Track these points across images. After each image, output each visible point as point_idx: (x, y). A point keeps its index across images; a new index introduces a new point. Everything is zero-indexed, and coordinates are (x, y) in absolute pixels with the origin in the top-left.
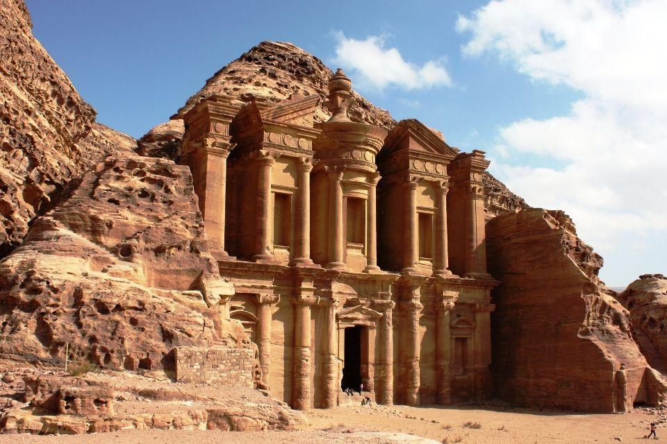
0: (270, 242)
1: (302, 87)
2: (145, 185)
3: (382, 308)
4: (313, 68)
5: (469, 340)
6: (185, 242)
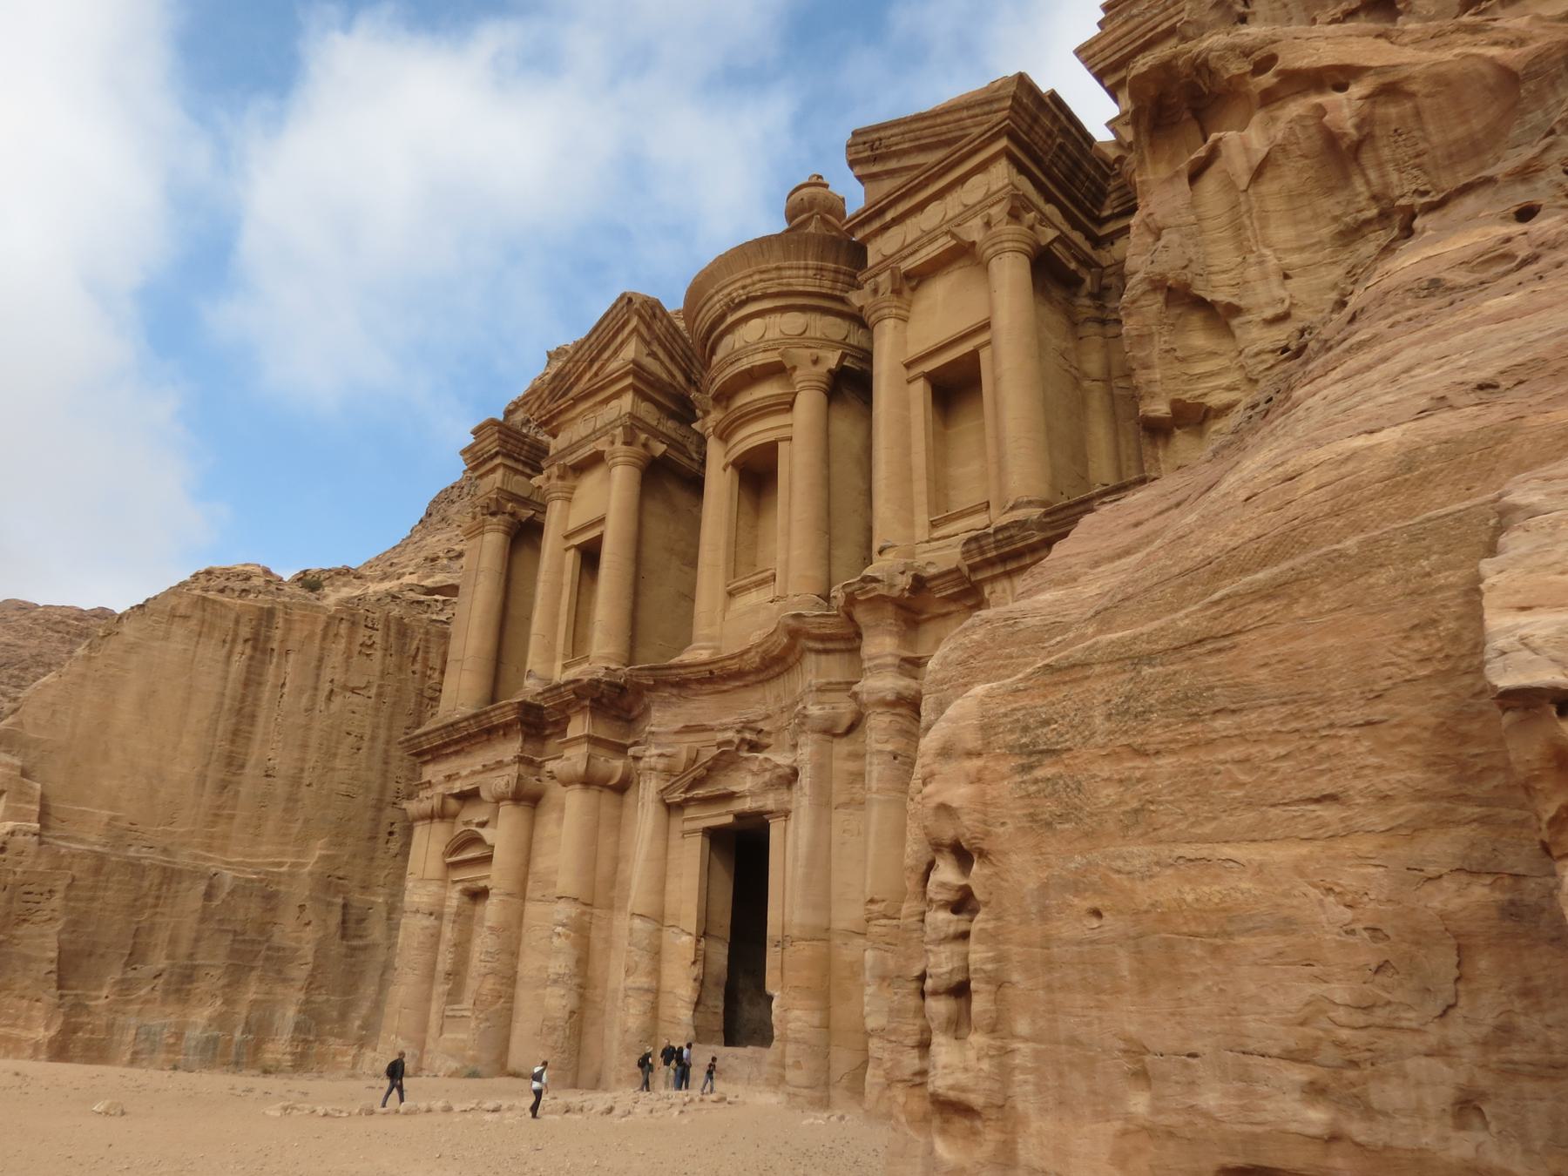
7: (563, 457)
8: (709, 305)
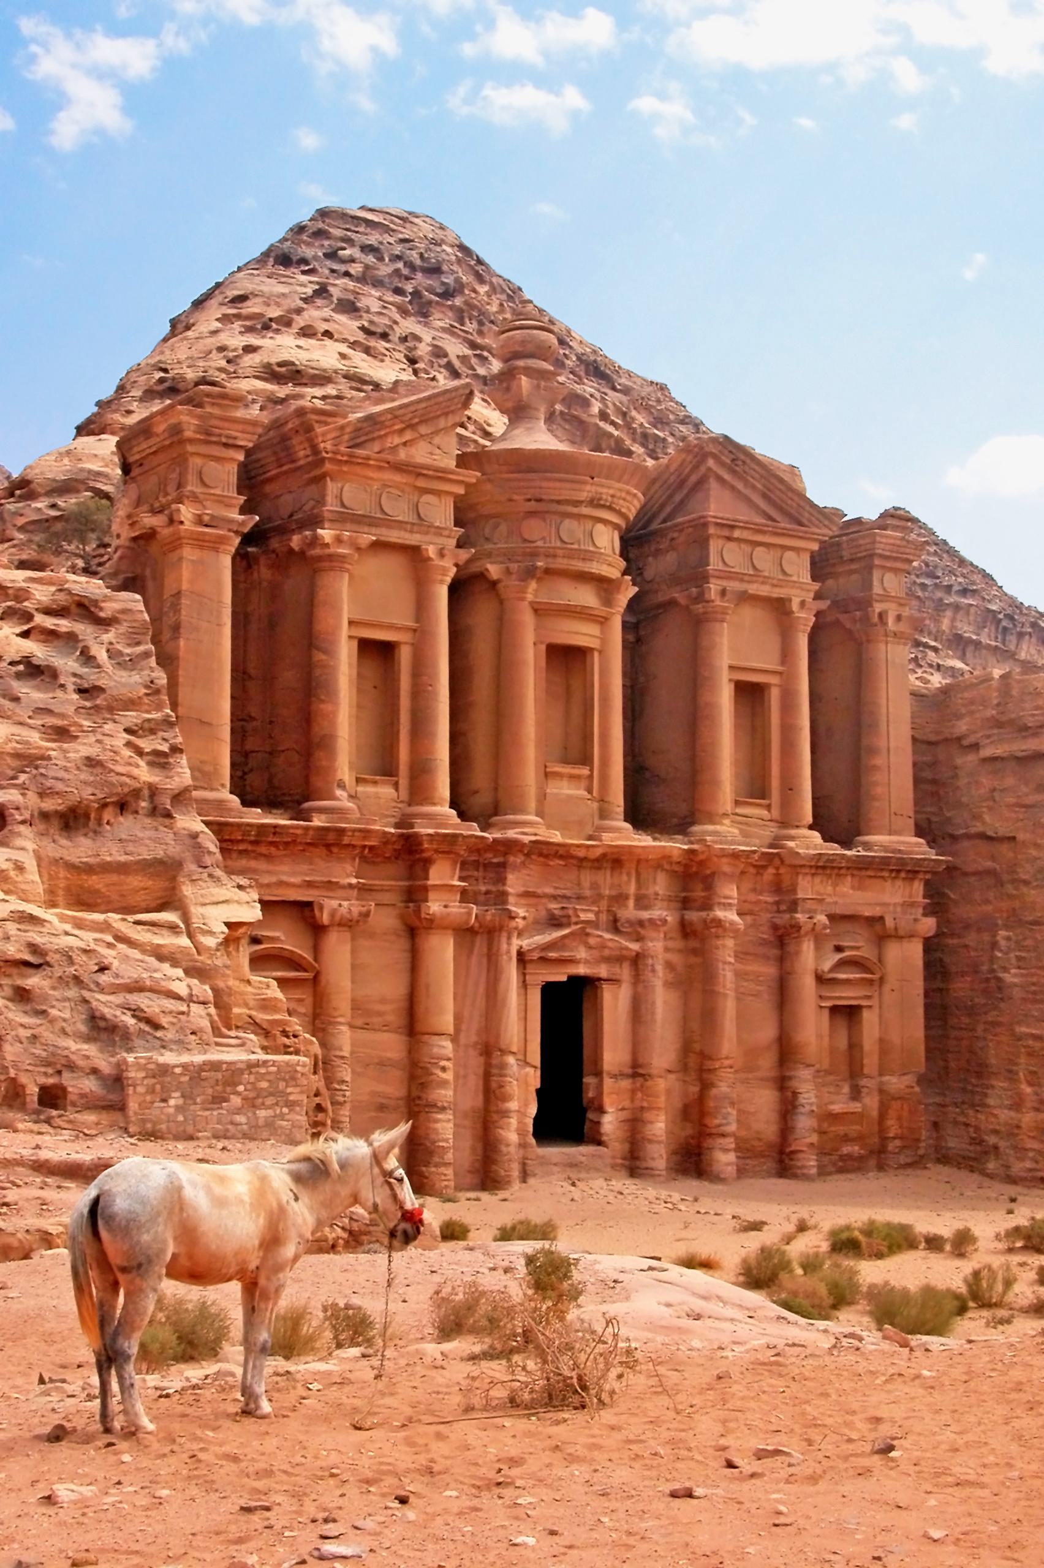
0: (346, 769)
1: (427, 336)
2: (33, 648)
3: (638, 929)
4: (458, 280)
5: (866, 1014)
6: (136, 793)
7: (359, 523)
8: (577, 486)
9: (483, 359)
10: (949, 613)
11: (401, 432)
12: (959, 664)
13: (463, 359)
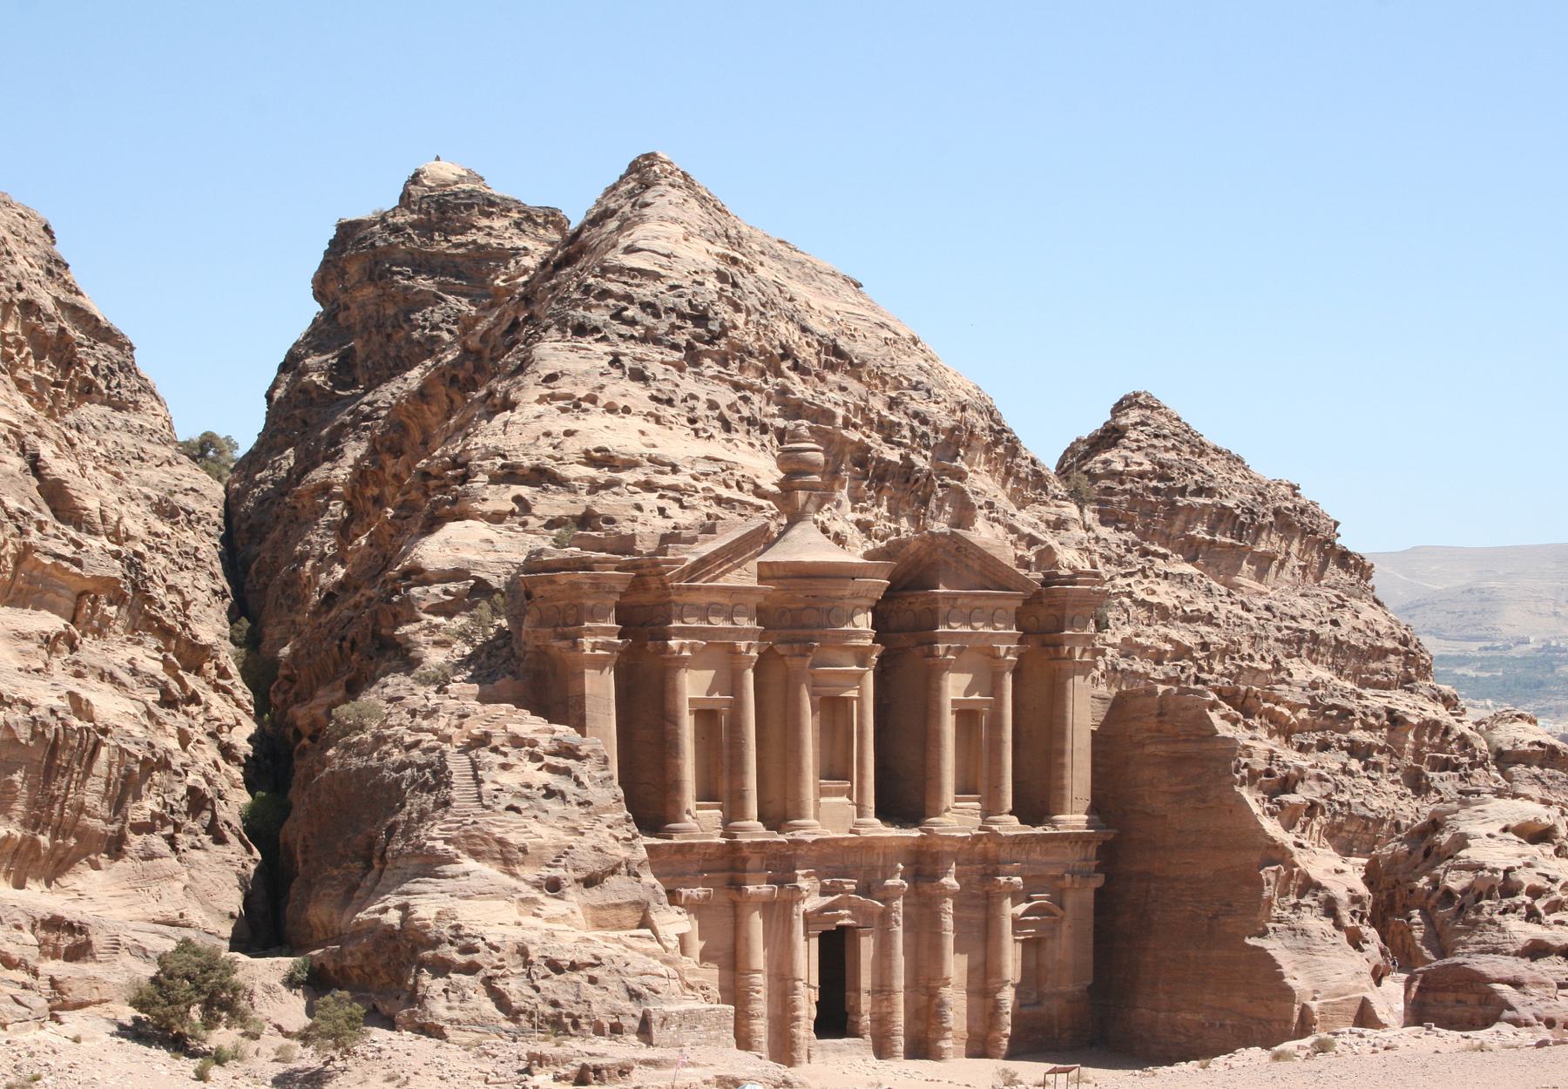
1: (703, 397)
2: (546, 777)
6: (619, 865)
9: (746, 399)
10: (1182, 517)
11: (720, 565)
12: (1188, 569)
13: (730, 407)
